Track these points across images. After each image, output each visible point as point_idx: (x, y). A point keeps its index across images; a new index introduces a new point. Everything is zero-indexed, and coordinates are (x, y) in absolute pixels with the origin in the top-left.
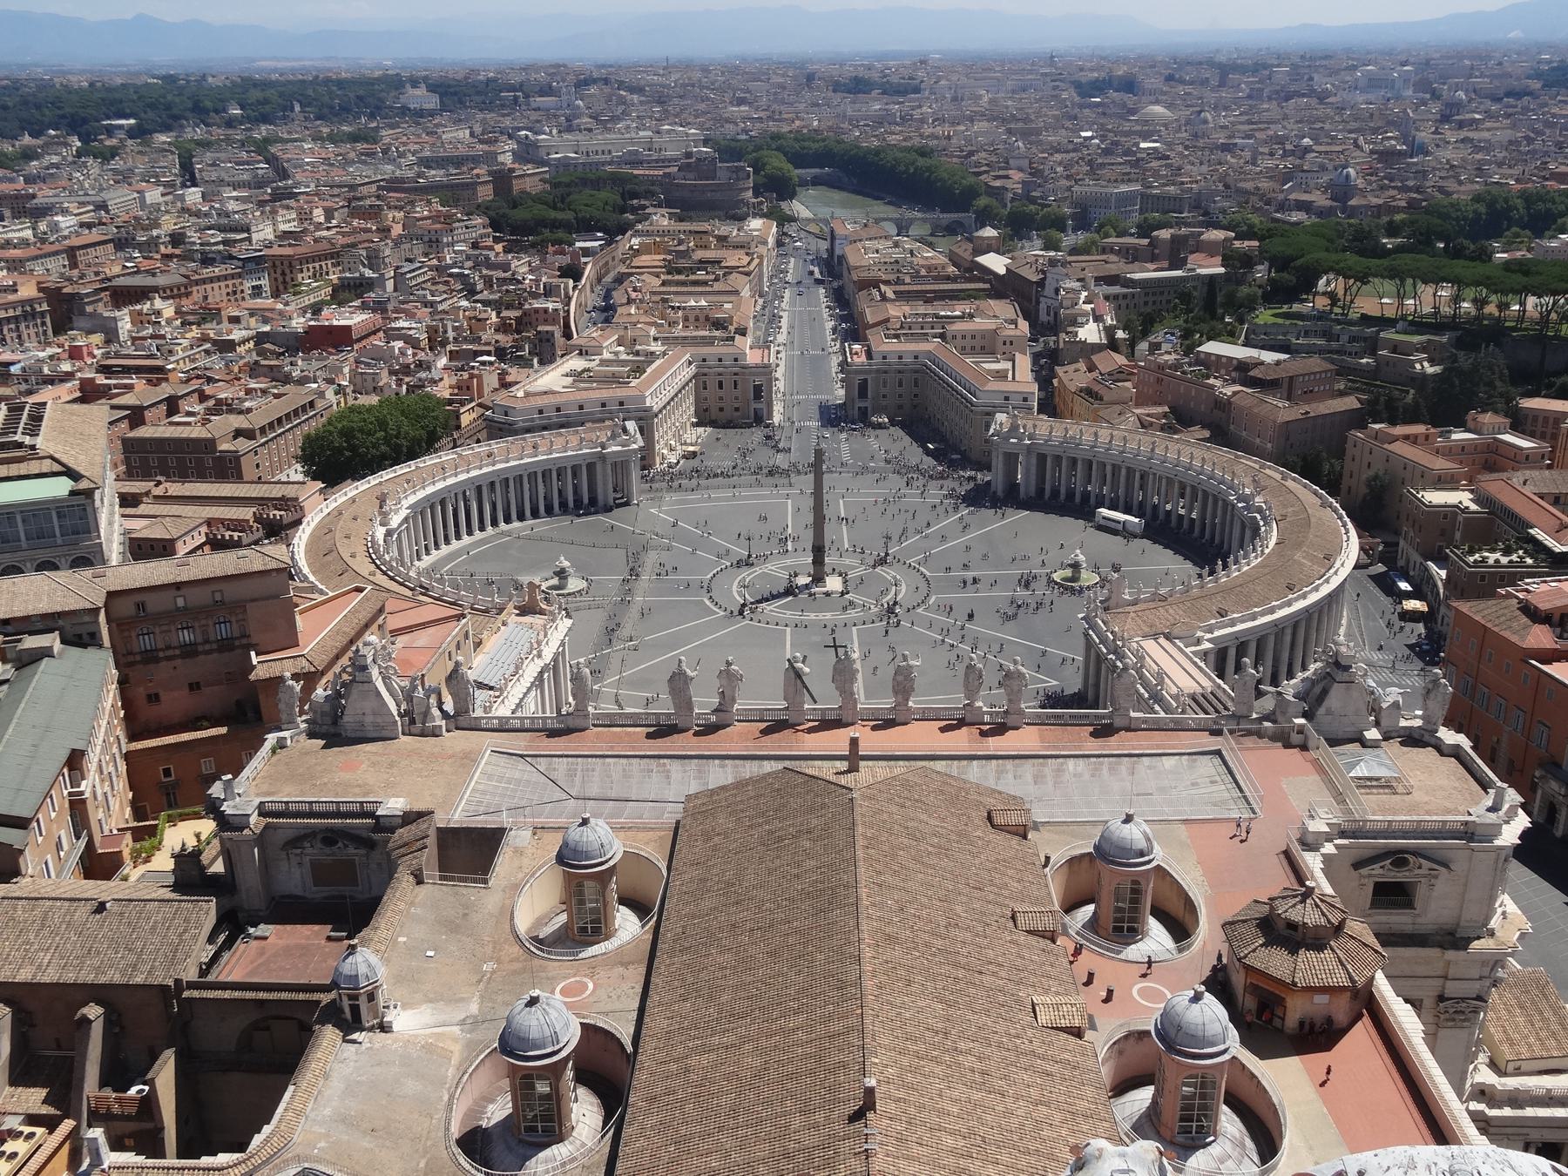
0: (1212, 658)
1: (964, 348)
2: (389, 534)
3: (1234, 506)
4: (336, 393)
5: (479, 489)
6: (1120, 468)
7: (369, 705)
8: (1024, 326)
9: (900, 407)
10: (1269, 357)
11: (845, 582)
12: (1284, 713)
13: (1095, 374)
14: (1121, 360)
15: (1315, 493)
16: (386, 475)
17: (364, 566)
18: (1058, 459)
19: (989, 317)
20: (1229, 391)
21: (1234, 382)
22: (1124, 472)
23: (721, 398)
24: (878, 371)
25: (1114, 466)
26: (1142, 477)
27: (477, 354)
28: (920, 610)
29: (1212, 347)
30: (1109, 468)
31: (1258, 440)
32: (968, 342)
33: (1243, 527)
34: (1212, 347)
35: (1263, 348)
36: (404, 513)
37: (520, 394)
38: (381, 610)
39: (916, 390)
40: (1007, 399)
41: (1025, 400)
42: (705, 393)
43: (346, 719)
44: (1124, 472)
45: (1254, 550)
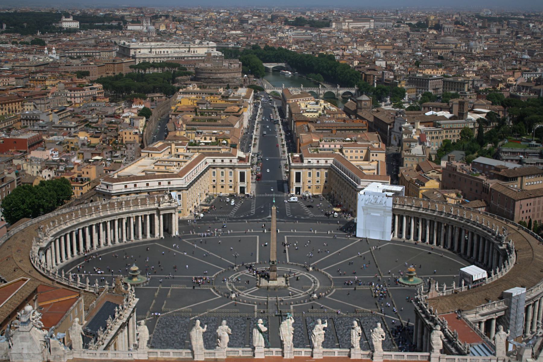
0: (483, 325)
1: (351, 157)
2: (41, 249)
3: (493, 243)
4: (17, 174)
5: (91, 227)
6: (434, 222)
7: (25, 344)
8: (382, 146)
9: (318, 187)
10: (511, 165)
11: (287, 280)
12: (521, 356)
13: (420, 173)
14: (434, 165)
15: (536, 238)
16: (42, 218)
17: (26, 267)
20: (492, 183)
21: (491, 177)
22: (436, 224)
23: (223, 181)
24: (306, 168)
25: (430, 221)
26: (445, 227)
27: (93, 154)
28: (327, 297)
29: (481, 160)
30: (428, 222)
31: (505, 209)
32: (354, 154)
33: (498, 254)
34: (481, 160)
35: (507, 160)
36: (50, 239)
37: (116, 177)
38: (35, 291)
43: (13, 351)
44: (436, 224)
45: (504, 267)
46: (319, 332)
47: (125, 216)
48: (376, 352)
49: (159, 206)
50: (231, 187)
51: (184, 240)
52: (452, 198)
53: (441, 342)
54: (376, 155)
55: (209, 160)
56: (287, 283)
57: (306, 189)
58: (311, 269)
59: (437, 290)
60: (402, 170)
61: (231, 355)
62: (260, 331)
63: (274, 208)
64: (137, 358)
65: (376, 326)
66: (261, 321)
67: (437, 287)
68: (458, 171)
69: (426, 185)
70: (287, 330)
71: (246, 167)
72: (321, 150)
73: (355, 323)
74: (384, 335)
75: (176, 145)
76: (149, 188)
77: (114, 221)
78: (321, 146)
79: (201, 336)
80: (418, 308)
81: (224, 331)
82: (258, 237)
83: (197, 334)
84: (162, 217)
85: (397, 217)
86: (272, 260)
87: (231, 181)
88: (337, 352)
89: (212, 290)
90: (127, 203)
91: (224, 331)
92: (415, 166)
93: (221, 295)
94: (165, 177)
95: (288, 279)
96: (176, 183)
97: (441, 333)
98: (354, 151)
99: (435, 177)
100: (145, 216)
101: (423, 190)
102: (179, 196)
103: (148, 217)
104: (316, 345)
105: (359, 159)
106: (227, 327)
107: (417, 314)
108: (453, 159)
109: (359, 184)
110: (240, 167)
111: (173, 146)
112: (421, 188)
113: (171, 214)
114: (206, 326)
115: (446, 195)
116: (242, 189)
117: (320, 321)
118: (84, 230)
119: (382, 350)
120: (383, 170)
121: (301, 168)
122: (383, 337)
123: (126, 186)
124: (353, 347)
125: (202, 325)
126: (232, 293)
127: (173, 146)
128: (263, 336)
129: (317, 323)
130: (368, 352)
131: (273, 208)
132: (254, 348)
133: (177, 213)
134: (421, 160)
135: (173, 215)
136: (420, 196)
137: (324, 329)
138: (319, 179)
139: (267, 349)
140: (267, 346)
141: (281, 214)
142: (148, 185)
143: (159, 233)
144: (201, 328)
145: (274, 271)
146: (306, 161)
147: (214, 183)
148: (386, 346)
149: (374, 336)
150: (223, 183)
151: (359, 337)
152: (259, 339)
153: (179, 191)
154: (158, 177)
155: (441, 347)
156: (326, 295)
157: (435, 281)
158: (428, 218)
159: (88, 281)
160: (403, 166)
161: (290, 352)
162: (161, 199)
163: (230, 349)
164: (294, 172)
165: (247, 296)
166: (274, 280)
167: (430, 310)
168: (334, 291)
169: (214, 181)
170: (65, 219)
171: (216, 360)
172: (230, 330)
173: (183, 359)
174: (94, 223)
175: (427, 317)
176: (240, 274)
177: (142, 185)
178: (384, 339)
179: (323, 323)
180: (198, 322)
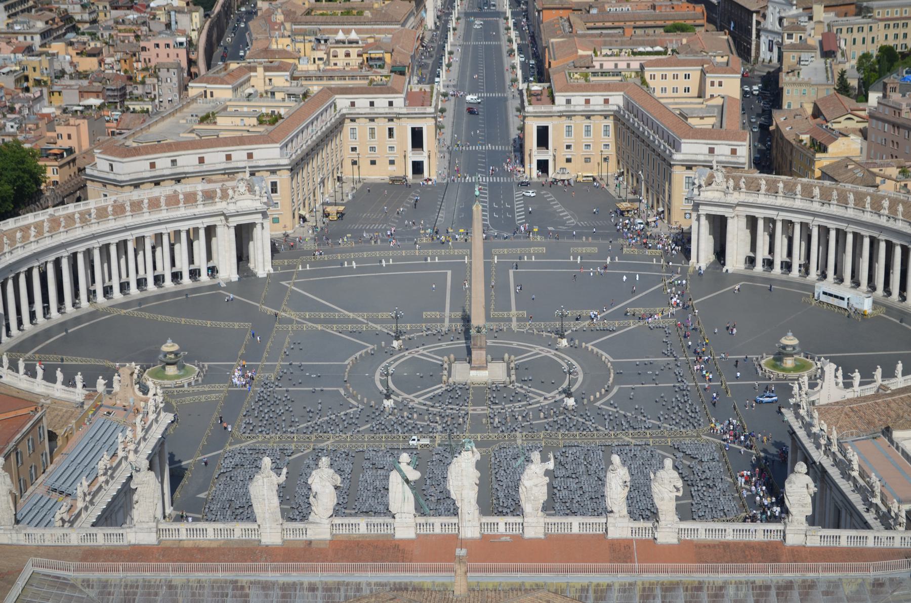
1: (664, 90)
5: (73, 258)
6: (845, 233)
8: (736, 60)
9: (587, 160)
11: (509, 369)
14: (849, 102)
18: (770, 222)
19: (696, 53)
22: (850, 238)
23: (373, 149)
27: (83, 93)
28: (598, 404)
30: (833, 235)
32: (670, 83)
40: (712, 151)
41: (734, 152)
44: (850, 238)
46: (534, 482)
47: (149, 233)
50: (392, 162)
51: (284, 283)
52: (890, 178)
53: (809, 500)
54: (720, 84)
55: (343, 102)
56: (509, 375)
57: (561, 163)
59: (841, 385)
60: (779, 118)
61: (344, 531)
62: (407, 481)
63: (477, 209)
64: (133, 542)
66: (405, 457)
67: (840, 379)
68: (904, 115)
69: (831, 148)
70: (463, 476)
71: (423, 116)
72: (595, 74)
73: (616, 459)
74: (680, 484)
75: (267, 69)
76: (204, 168)
77: (125, 242)
78: (597, 66)
79: (275, 492)
80: (796, 425)
81: (323, 483)
82: (449, 272)
83: (264, 489)
84: (232, 231)
85: (761, 224)
87: (391, 148)
88: (575, 525)
89: (342, 392)
90: (154, 204)
91: (323, 483)
92: (809, 109)
93: (361, 402)
94: (240, 141)
95: (512, 365)
97: (808, 480)
98: (670, 75)
99: (854, 131)
100: (196, 230)
101: (822, 161)
102: (274, 184)
103: (202, 233)
104: (527, 507)
105: (681, 93)
107: (793, 439)
108: (894, 90)
109: (678, 150)
110: (409, 116)
111: (260, 70)
112: (818, 155)
113: (253, 225)
114: (285, 471)
115: (876, 170)
116: (418, 167)
117: (536, 456)
118: (57, 263)
119: (676, 519)
120: (734, 118)
121: (549, 116)
122: (678, 490)
123: (153, 165)
125: (277, 469)
126: (388, 397)
127: (260, 70)
128: (412, 488)
129: (528, 460)
130: (642, 524)
131: (474, 208)
132: (394, 517)
133: (267, 223)
134: (823, 94)
135: (259, 227)
136: (818, 173)
137: (547, 473)
138: (586, 140)
139: (422, 520)
140: (420, 510)
141: (502, 223)
142: (201, 160)
143: (228, 271)
144: (272, 474)
145: (481, 348)
146: (560, 99)
147: (354, 156)
149: (656, 488)
150: (373, 156)
151: (627, 489)
152: (400, 497)
153: (273, 172)
155: (809, 511)
156: (596, 400)
157: (834, 366)
158: (832, 225)
159: (60, 375)
160: (779, 106)
161: (471, 524)
162: (230, 192)
163: (337, 521)
164: (532, 127)
165: (420, 403)
168: (615, 390)
169: (354, 149)
170: (13, 241)
171: (310, 542)
173: (236, 541)
174: (81, 248)
175: (818, 447)
176: (407, 355)
177: (187, 161)
178: (680, 494)
179: (544, 459)
180: (267, 461)
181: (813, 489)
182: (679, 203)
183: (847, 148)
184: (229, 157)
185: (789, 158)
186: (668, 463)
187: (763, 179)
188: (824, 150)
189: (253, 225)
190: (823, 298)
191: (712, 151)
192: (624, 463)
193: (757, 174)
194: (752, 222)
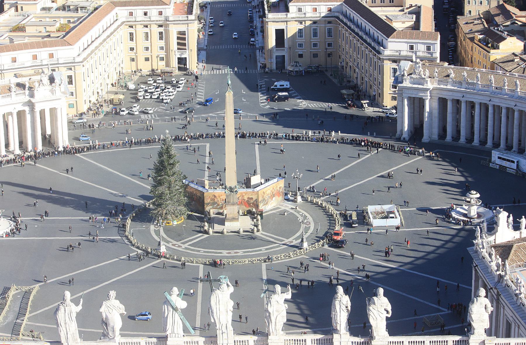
6: (513, 111)
9: (315, 55)
18: (458, 102)
22: (516, 114)
30: (504, 111)
39: (330, 40)
40: (412, 48)
42: (132, 44)
44: (516, 114)
48: (377, 337)
49: (32, 95)
50: (162, 59)
55: (122, 13)
58: (299, 199)
65: (376, 295)
69: (502, 45)
71: (187, 22)
74: (389, 308)
76: (16, 65)
86: (228, 185)
87: (162, 48)
96: (64, 53)
97: (487, 301)
101: (495, 55)
102: (70, 77)
106: (118, 301)
110: (176, 22)
112: (492, 51)
120: (428, 22)
122: (388, 312)
124: (336, 331)
138: (314, 40)
142: (14, 60)
144: (73, 305)
145: (233, 204)
147: (132, 54)
148: (395, 327)
150: (148, 54)
154: (31, 46)
155: (487, 325)
160: (462, 14)
162: (37, 84)
165: (186, 248)
166: (234, 219)
167: (498, 266)
169: (132, 49)
172: (122, 307)
178: (389, 316)
180: (68, 294)
181: (490, 309)
182: (388, 91)
183: (512, 45)
184: (35, 57)
185: (471, 53)
186: (381, 291)
187: (452, 70)
188: (498, 48)
189: (53, 111)
190: (498, 162)
191: (412, 48)
192: (346, 292)
193: (446, 64)
194: (443, 102)
